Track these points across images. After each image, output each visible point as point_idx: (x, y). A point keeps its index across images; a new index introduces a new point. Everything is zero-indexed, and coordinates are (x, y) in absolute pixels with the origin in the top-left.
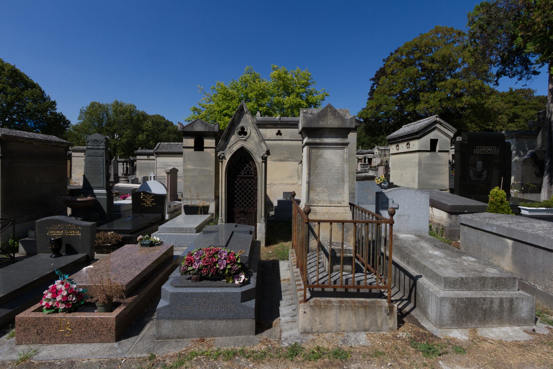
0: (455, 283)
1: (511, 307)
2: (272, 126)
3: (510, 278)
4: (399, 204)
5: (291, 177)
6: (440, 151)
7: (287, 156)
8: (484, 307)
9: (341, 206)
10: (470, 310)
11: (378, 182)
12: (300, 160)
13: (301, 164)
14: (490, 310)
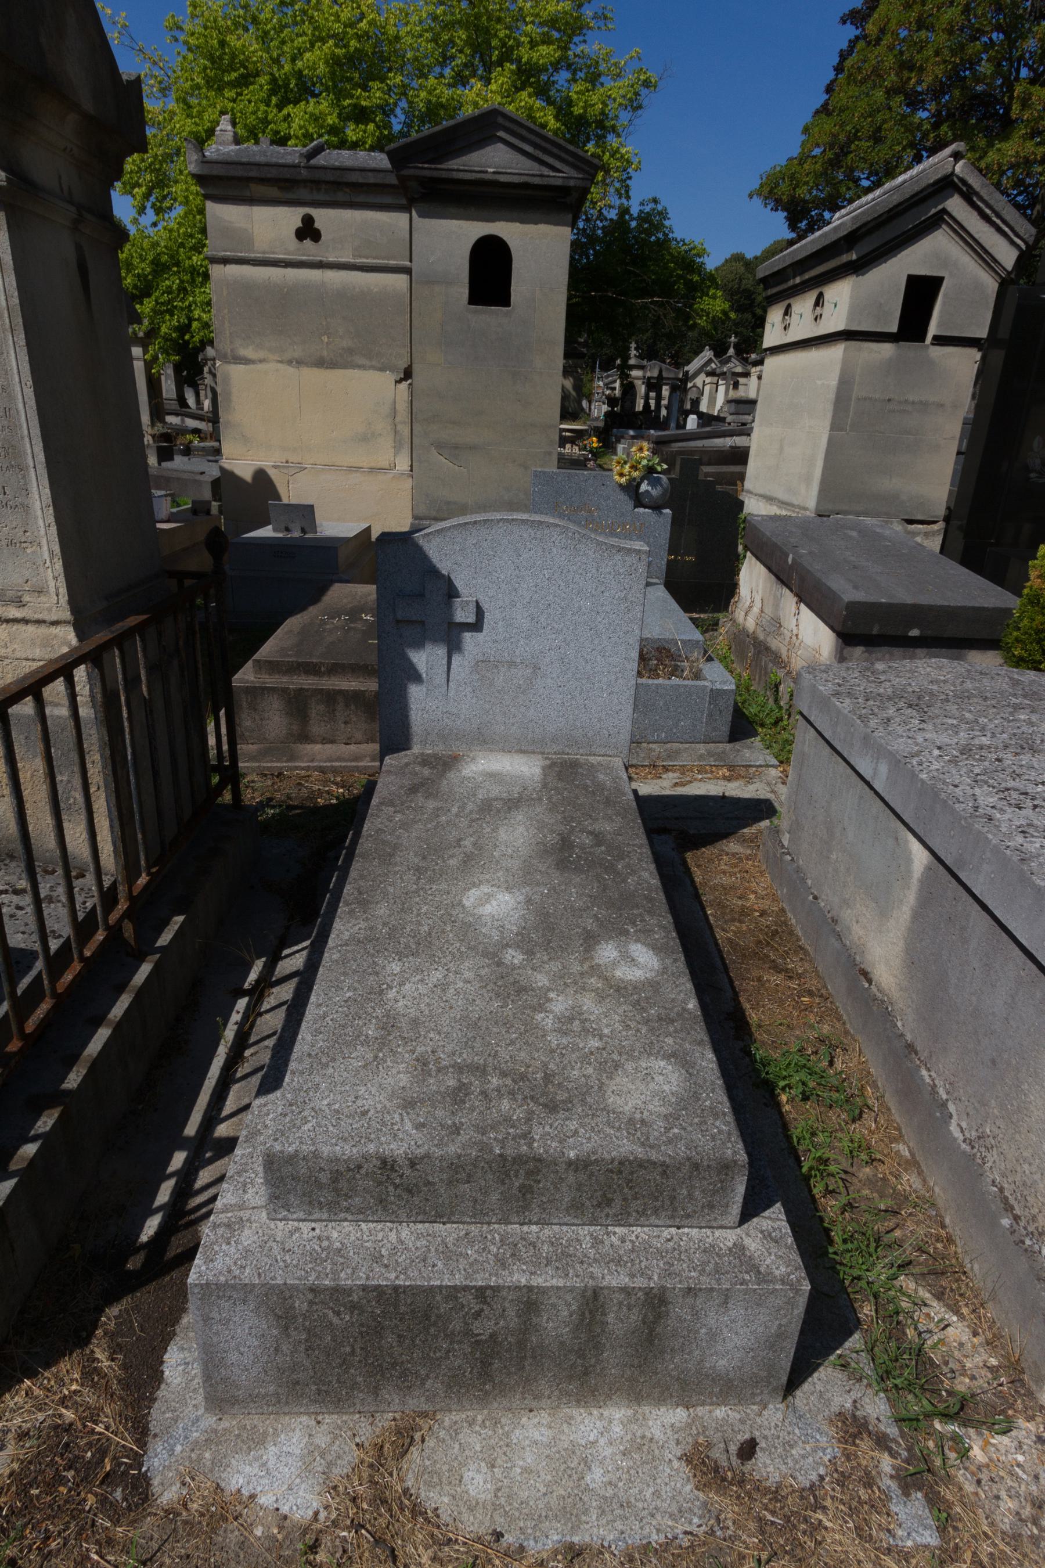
0: (343, 1184)
1: (652, 1330)
2: (273, 192)
3: (696, 1166)
4: (485, 606)
5: (366, 438)
6: (411, 261)
7: (346, 343)
8: (483, 1328)
9: (25, 621)
10: (390, 1338)
11: (621, 475)
12: (403, 364)
13: (404, 385)
14: (521, 1344)
